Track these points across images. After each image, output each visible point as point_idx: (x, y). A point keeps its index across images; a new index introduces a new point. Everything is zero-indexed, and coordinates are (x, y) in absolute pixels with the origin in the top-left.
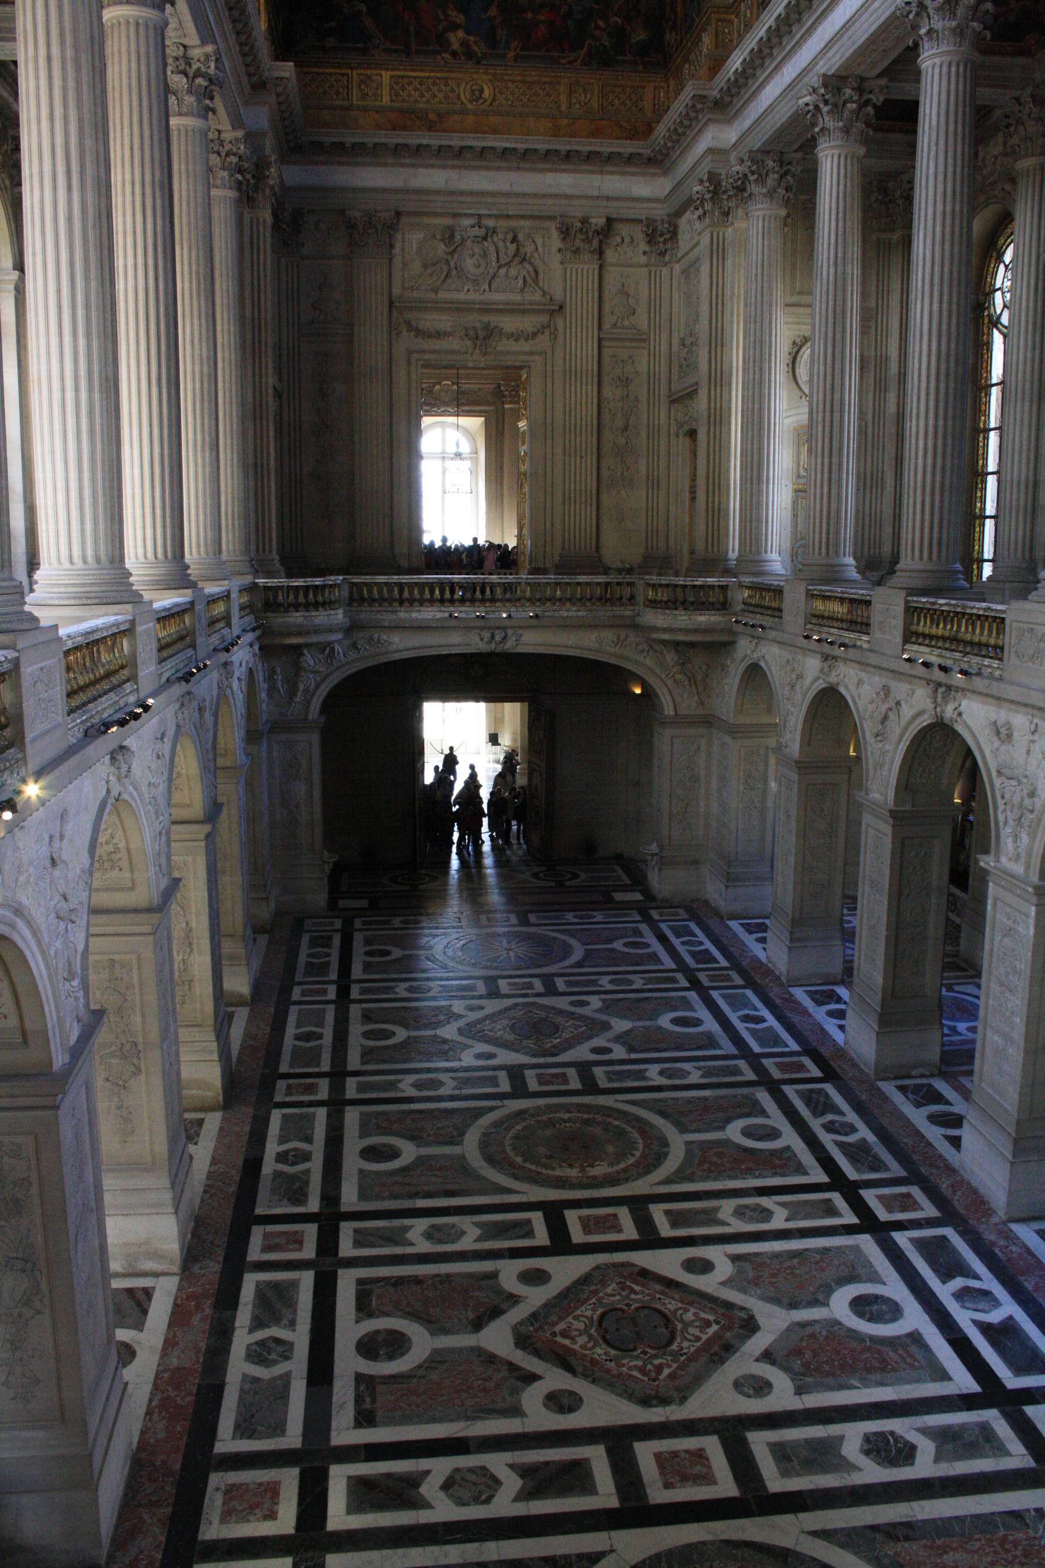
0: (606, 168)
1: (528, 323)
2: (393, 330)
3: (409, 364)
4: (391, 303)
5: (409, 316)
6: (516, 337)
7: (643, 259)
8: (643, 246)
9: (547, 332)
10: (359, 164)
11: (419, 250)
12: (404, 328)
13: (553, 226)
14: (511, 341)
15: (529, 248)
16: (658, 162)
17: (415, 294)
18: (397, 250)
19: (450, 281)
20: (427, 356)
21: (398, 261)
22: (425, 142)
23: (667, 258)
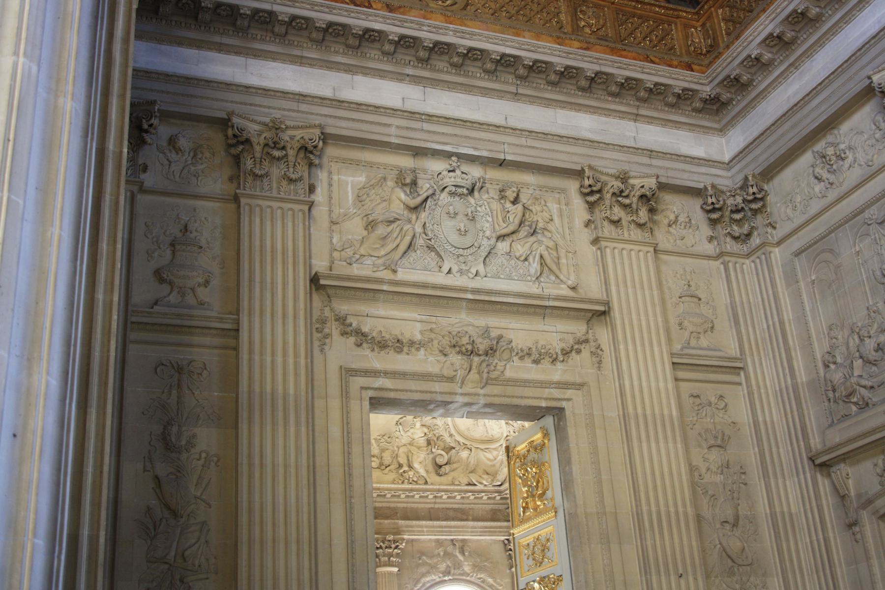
0: (642, 112)
1: (554, 333)
2: (318, 329)
3: (345, 394)
4: (315, 280)
5: (343, 307)
6: (537, 356)
7: (710, 248)
8: (706, 230)
9: (586, 353)
10: (257, 54)
11: (359, 199)
12: (334, 329)
13: (573, 186)
14: (528, 363)
15: (539, 217)
16: (716, 108)
17: (356, 270)
18: (319, 196)
19: (412, 255)
20: (380, 382)
21: (321, 212)
22: (377, 26)
23: (756, 241)
